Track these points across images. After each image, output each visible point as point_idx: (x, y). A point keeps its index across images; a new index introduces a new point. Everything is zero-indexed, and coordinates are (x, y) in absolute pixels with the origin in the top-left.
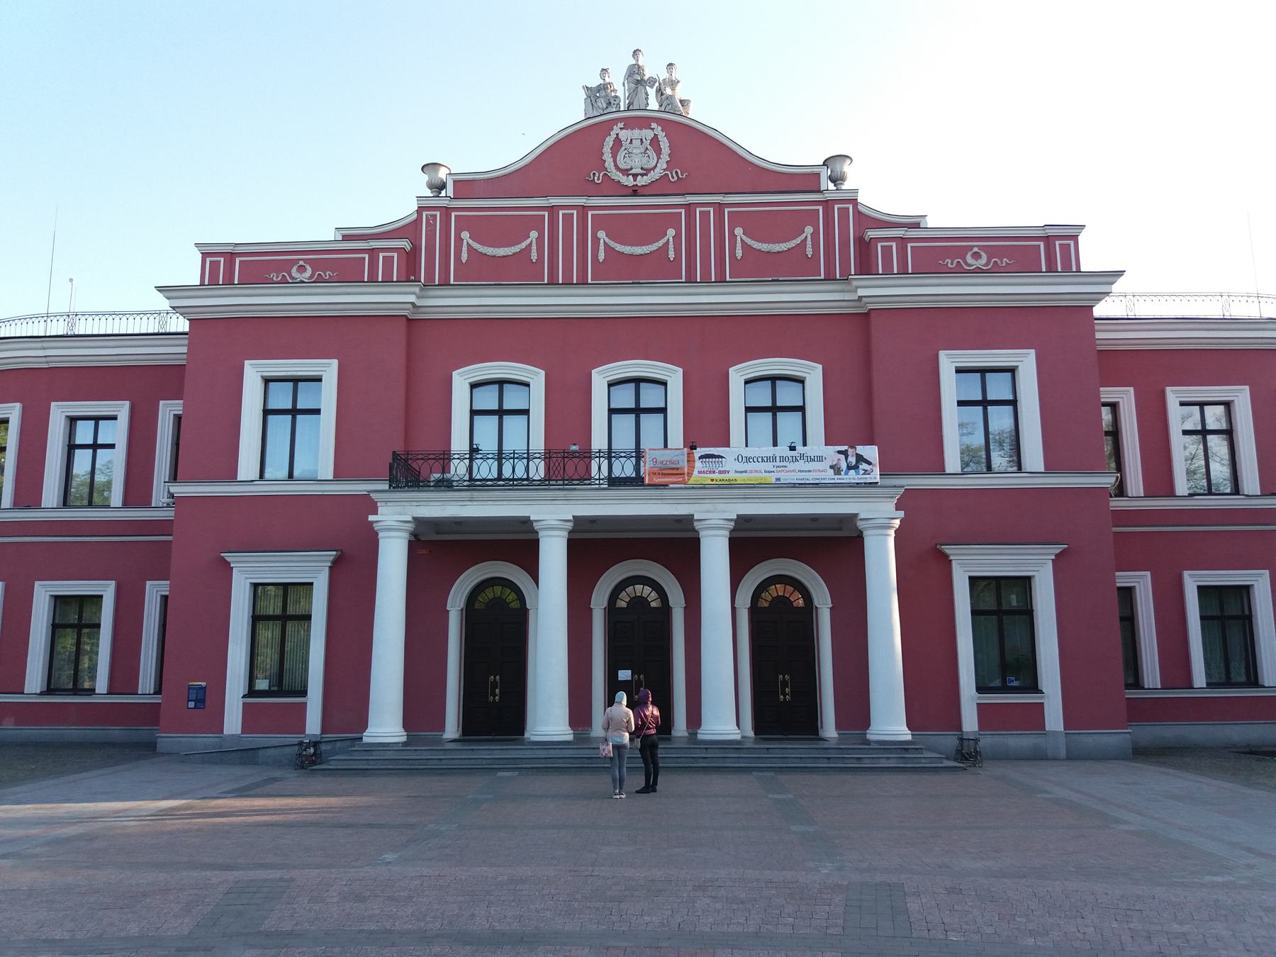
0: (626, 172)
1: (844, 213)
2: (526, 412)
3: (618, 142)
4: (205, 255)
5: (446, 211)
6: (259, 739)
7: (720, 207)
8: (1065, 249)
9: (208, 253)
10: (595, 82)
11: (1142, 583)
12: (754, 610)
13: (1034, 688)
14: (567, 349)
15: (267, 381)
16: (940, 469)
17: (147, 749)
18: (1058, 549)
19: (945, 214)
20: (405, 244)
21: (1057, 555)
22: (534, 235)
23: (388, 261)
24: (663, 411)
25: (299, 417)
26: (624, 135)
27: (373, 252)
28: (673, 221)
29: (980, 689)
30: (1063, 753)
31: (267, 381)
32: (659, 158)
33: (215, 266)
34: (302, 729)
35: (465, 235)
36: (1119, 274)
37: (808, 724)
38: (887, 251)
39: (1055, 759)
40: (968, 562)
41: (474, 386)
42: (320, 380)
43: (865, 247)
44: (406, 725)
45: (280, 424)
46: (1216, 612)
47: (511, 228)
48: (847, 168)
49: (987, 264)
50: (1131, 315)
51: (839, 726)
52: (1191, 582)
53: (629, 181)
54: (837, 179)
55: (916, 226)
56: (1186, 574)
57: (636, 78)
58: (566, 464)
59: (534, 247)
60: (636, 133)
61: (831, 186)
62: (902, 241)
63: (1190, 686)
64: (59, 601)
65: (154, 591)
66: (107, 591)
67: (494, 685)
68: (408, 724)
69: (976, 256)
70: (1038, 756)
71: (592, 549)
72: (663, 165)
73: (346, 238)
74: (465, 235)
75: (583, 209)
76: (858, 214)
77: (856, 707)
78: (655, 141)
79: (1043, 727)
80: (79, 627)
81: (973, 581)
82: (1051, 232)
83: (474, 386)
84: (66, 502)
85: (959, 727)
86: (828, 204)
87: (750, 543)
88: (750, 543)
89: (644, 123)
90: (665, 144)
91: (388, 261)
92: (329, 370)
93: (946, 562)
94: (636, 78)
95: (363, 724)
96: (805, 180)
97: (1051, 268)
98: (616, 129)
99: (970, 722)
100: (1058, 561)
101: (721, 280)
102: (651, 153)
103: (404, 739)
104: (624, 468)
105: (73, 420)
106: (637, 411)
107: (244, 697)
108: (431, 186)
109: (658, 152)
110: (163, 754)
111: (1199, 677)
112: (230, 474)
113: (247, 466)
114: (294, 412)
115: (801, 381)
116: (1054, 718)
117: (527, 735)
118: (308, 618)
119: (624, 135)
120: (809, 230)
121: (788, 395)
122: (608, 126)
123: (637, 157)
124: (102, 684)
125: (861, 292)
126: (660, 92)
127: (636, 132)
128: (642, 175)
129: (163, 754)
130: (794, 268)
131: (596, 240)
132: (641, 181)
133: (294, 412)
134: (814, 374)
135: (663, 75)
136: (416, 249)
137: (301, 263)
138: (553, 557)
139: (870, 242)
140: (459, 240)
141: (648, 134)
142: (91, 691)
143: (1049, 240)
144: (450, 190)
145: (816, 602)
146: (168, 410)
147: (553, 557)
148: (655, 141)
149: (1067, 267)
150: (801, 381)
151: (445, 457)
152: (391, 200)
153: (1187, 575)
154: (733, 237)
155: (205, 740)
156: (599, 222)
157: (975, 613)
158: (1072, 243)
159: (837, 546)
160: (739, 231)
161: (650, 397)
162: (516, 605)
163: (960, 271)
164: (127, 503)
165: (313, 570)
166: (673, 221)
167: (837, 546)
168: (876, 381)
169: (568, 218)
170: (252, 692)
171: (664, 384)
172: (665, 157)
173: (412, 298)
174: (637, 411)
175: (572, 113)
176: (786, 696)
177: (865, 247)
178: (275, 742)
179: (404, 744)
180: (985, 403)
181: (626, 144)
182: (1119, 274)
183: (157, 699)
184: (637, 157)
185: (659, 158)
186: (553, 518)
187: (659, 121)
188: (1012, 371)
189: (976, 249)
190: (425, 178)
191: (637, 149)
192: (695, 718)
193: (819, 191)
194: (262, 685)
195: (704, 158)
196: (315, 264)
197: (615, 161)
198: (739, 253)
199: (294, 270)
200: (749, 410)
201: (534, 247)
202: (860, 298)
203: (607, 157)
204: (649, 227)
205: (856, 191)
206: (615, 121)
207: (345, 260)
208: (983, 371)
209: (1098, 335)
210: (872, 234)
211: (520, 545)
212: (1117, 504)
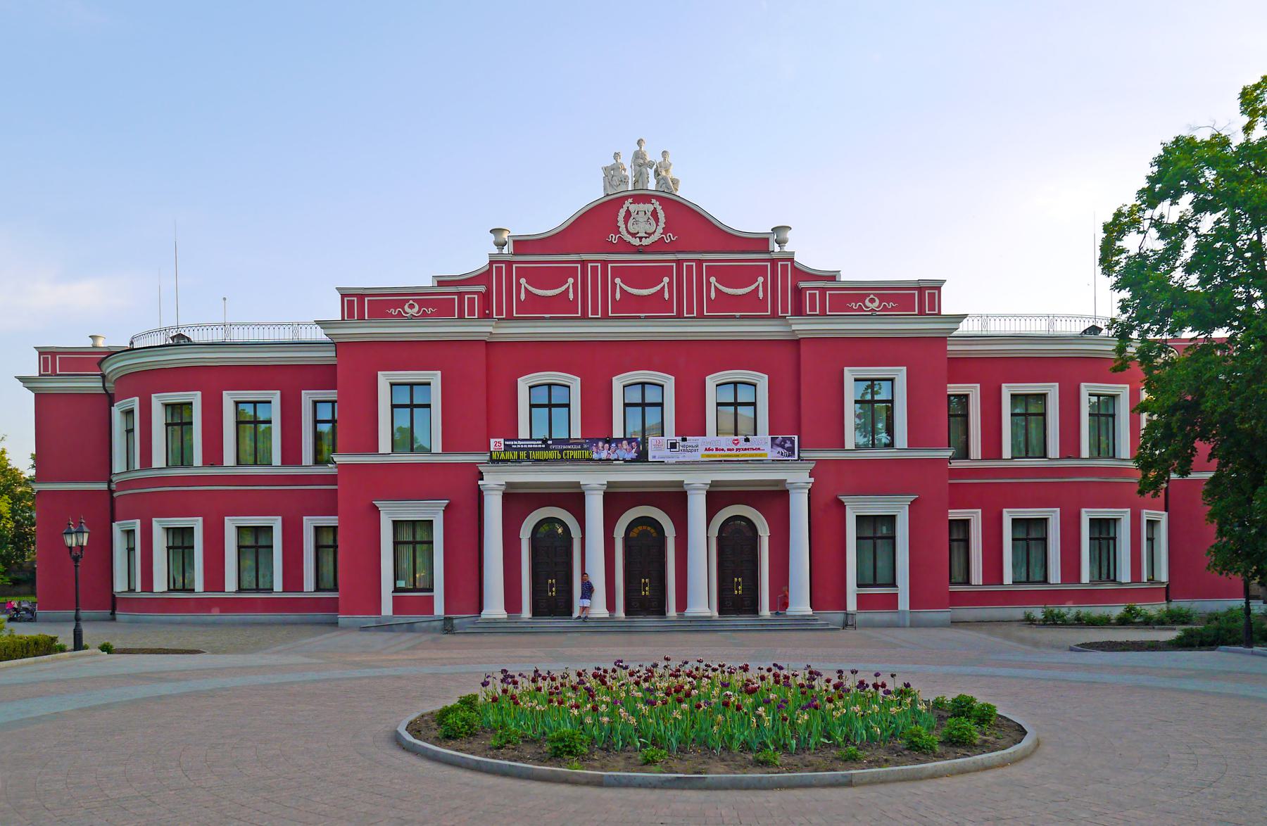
0: (634, 235)
1: (784, 268)
5: (509, 264)
6: (402, 619)
9: (345, 295)
12: (719, 539)
13: (894, 585)
14: (595, 363)
19: (852, 273)
20: (482, 289)
22: (571, 280)
23: (471, 301)
24: (661, 405)
26: (633, 208)
27: (461, 295)
28: (667, 271)
29: (858, 586)
30: (908, 623)
31: (392, 385)
34: (432, 612)
35: (523, 281)
38: (813, 297)
39: (904, 627)
41: (530, 387)
43: (798, 292)
44: (507, 609)
46: (1023, 536)
47: (555, 276)
48: (789, 234)
50: (984, 333)
53: (636, 242)
54: (781, 243)
55: (832, 277)
57: (640, 160)
59: (571, 290)
60: (642, 207)
61: (777, 248)
62: (823, 290)
67: (552, 585)
69: (872, 301)
71: (616, 501)
72: (660, 230)
73: (442, 283)
74: (523, 281)
75: (605, 263)
76: (794, 268)
81: (859, 519)
85: (845, 608)
86: (774, 262)
87: (717, 498)
88: (717, 498)
90: (661, 215)
91: (471, 301)
92: (435, 378)
93: (842, 506)
94: (640, 160)
96: (759, 243)
98: (627, 204)
99: (852, 605)
100: (913, 505)
108: (497, 244)
109: (657, 220)
112: (374, 448)
116: (904, 603)
119: (633, 208)
120: (761, 279)
121: (745, 395)
122: (620, 201)
123: (643, 225)
125: (794, 327)
126: (657, 173)
127: (641, 205)
129: (344, 628)
130: (750, 306)
131: (614, 285)
132: (646, 242)
134: (763, 381)
135: (660, 159)
136: (489, 291)
138: (595, 508)
140: (519, 285)
147: (595, 508)
148: (654, 213)
152: (472, 257)
154: (709, 283)
155: (370, 620)
156: (616, 272)
159: (773, 500)
165: (433, 511)
166: (667, 271)
167: (773, 500)
168: (803, 389)
170: (396, 590)
171: (662, 386)
172: (662, 225)
173: (490, 329)
175: (593, 192)
177: (798, 292)
181: (634, 215)
186: (594, 482)
187: (658, 198)
188: (892, 380)
191: (641, 217)
192: (682, 604)
193: (768, 252)
194: (401, 584)
195: (688, 223)
196: (422, 303)
200: (718, 404)
201: (571, 290)
203: (621, 224)
205: (793, 253)
206: (626, 198)
207: (442, 299)
210: (802, 285)
211: (574, 500)
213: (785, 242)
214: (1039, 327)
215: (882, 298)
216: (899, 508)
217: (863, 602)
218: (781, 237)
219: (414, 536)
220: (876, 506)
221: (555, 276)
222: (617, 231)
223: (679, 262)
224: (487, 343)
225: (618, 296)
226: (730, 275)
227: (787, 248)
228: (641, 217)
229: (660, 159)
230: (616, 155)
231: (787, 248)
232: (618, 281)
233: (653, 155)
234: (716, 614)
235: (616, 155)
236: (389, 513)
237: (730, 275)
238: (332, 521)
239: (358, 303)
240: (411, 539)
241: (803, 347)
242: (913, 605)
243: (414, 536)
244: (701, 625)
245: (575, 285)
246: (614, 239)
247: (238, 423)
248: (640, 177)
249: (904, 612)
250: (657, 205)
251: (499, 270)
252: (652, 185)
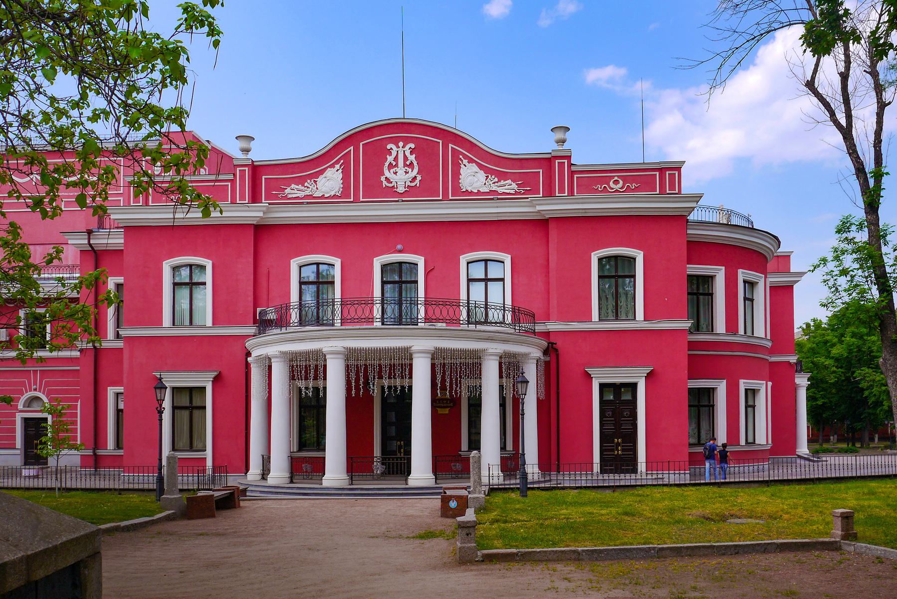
8: (672, 177)
49: (622, 188)
69: (616, 182)
121: (494, 271)
125: (538, 208)
143: (662, 171)
158: (677, 173)
173: (261, 214)
189: (616, 178)
202: (539, 211)
219: (191, 401)
238: (120, 389)
240: (188, 404)
241: (552, 226)
243: (191, 401)
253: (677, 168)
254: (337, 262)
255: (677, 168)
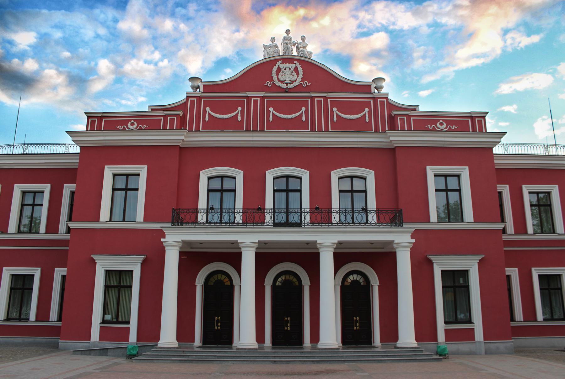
0: (282, 82)
2: (234, 191)
3: (279, 69)
4: (89, 118)
5: (199, 98)
7: (326, 98)
8: (480, 122)
9: (90, 116)
10: (268, 43)
11: (514, 273)
13: (470, 322)
14: (254, 161)
15: (115, 175)
16: (428, 221)
17: (55, 347)
18: (480, 257)
20: (180, 113)
21: (480, 260)
22: (240, 109)
23: (172, 120)
24: (300, 191)
25: (224, 193)
26: (282, 66)
27: (165, 117)
28: (305, 104)
29: (446, 323)
31: (115, 175)
32: (298, 76)
33: (93, 122)
34: (127, 339)
36: (505, 133)
37: (367, 340)
40: (441, 264)
41: (209, 178)
42: (139, 175)
45: (120, 195)
46: (546, 287)
47: (229, 106)
49: (446, 128)
50: (506, 153)
51: (381, 341)
52: (536, 273)
53: (284, 86)
55: (414, 110)
56: (533, 269)
57: (287, 41)
58: (254, 215)
59: (239, 115)
61: (376, 91)
62: (409, 116)
63: (536, 320)
64: (15, 277)
65: (59, 273)
66: (37, 272)
68: (179, 339)
70: (471, 353)
72: (299, 79)
73: (154, 109)
75: (263, 98)
77: (391, 332)
78: (296, 69)
79: (474, 340)
80: (23, 289)
82: (474, 115)
83: (209, 178)
84: (19, 231)
86: (375, 99)
89: (290, 60)
90: (300, 70)
91: (172, 120)
92: (143, 170)
95: (158, 338)
96: (365, 88)
97: (474, 130)
98: (278, 63)
100: (480, 263)
101: (327, 130)
102: (294, 74)
103: (177, 346)
104: (281, 218)
105: (24, 193)
106: (287, 191)
107: (100, 323)
108: (192, 87)
109: (298, 73)
110: (65, 349)
111: (540, 316)
113: (104, 214)
114: (126, 190)
115: (365, 179)
116: (479, 335)
117: (234, 345)
118: (131, 287)
119: (282, 66)
120: (367, 110)
121: (358, 185)
122: (273, 62)
123: (288, 76)
124: (33, 316)
125: (391, 138)
126: (297, 48)
128: (290, 83)
129: (62, 350)
130: (360, 126)
131: (269, 112)
132: (290, 86)
133: (126, 190)
134: (371, 176)
136: (185, 116)
137: (132, 121)
139: (394, 116)
141: (294, 66)
142: (28, 320)
143: (473, 118)
144: (201, 89)
145: (372, 283)
146: (68, 189)
148: (296, 69)
149: (481, 130)
150: (365, 179)
151: (196, 211)
153: (533, 269)
154: (332, 112)
155: (81, 344)
156: (270, 104)
157: (443, 287)
160: (335, 109)
161: (293, 184)
162: (229, 283)
163: (434, 130)
164: (47, 232)
165: (133, 264)
169: (256, 102)
170: (104, 322)
172: (301, 76)
173: (183, 137)
174: (287, 191)
176: (357, 327)
177: (392, 120)
178: (115, 346)
179: (177, 348)
180: (447, 190)
181: (283, 70)
182: (505, 133)
183: (59, 324)
184: (288, 76)
185: (298, 76)
187: (298, 60)
188: (458, 176)
189: (441, 121)
190: (190, 84)
191: (287, 71)
194: (108, 317)
197: (278, 77)
198: (335, 119)
199: (129, 125)
202: (391, 141)
204: (293, 106)
205: (387, 94)
207: (153, 119)
208: (446, 176)
209: (495, 161)
210: (395, 113)
212: (505, 237)
213: (382, 87)
214: (540, 151)
215: (448, 123)
216: (471, 265)
217: (450, 335)
218: (379, 84)
220: (455, 263)
221: (229, 106)
222: (271, 79)
223: (312, 98)
224: (181, 149)
225: (271, 119)
226: (344, 107)
227: (383, 91)
228: (287, 71)
229: (300, 41)
230: (273, 40)
231: (383, 91)
232: (271, 109)
233: (296, 39)
234: (341, 345)
235: (273, 40)
236: (104, 264)
237: (344, 107)
239: (96, 120)
242: (487, 336)
244: (329, 356)
245: (242, 112)
246: (269, 84)
247: (23, 205)
248: (287, 49)
249: (480, 342)
250: (298, 64)
251: (193, 102)
252: (295, 53)
253: (482, 116)
254: (240, 175)
255: (482, 116)
